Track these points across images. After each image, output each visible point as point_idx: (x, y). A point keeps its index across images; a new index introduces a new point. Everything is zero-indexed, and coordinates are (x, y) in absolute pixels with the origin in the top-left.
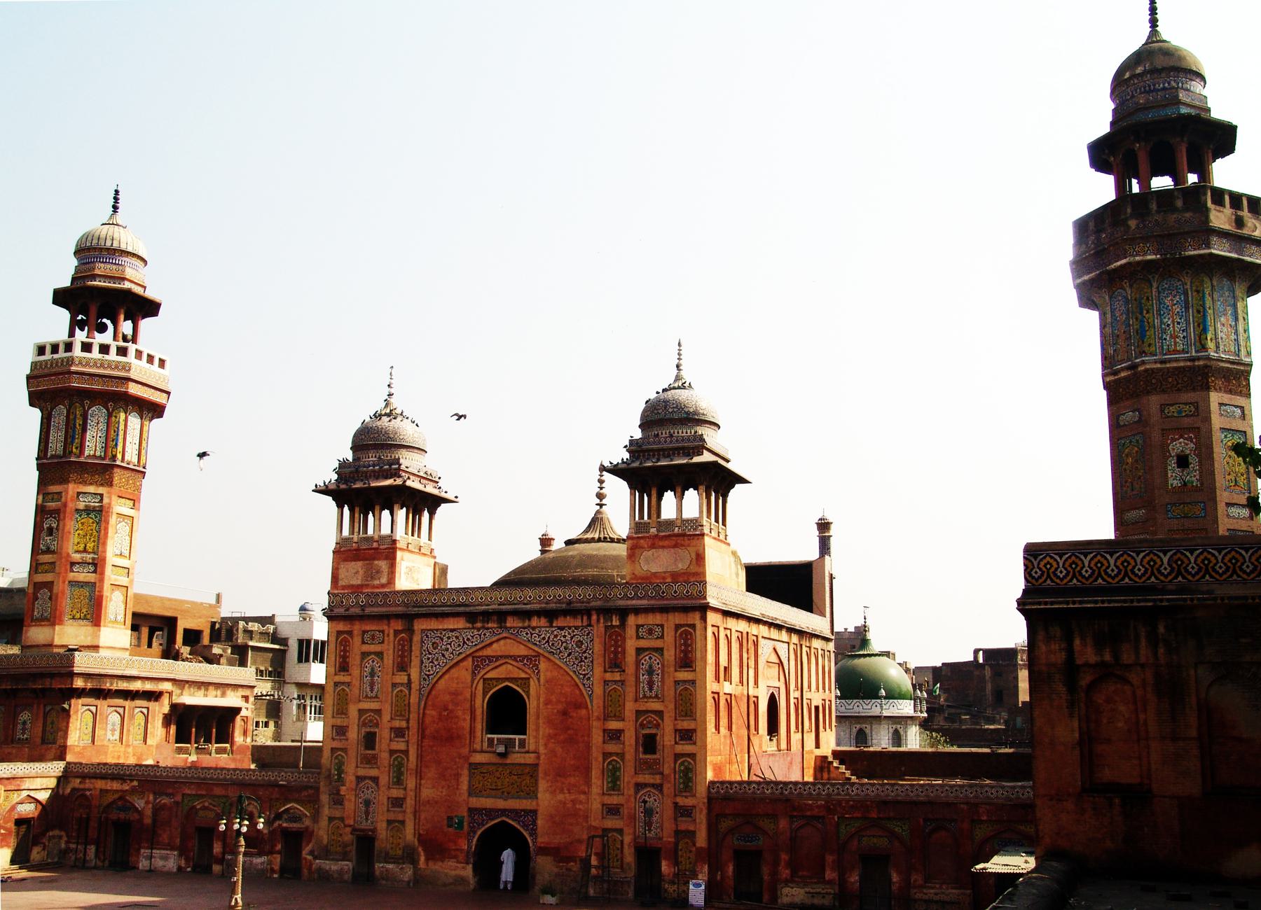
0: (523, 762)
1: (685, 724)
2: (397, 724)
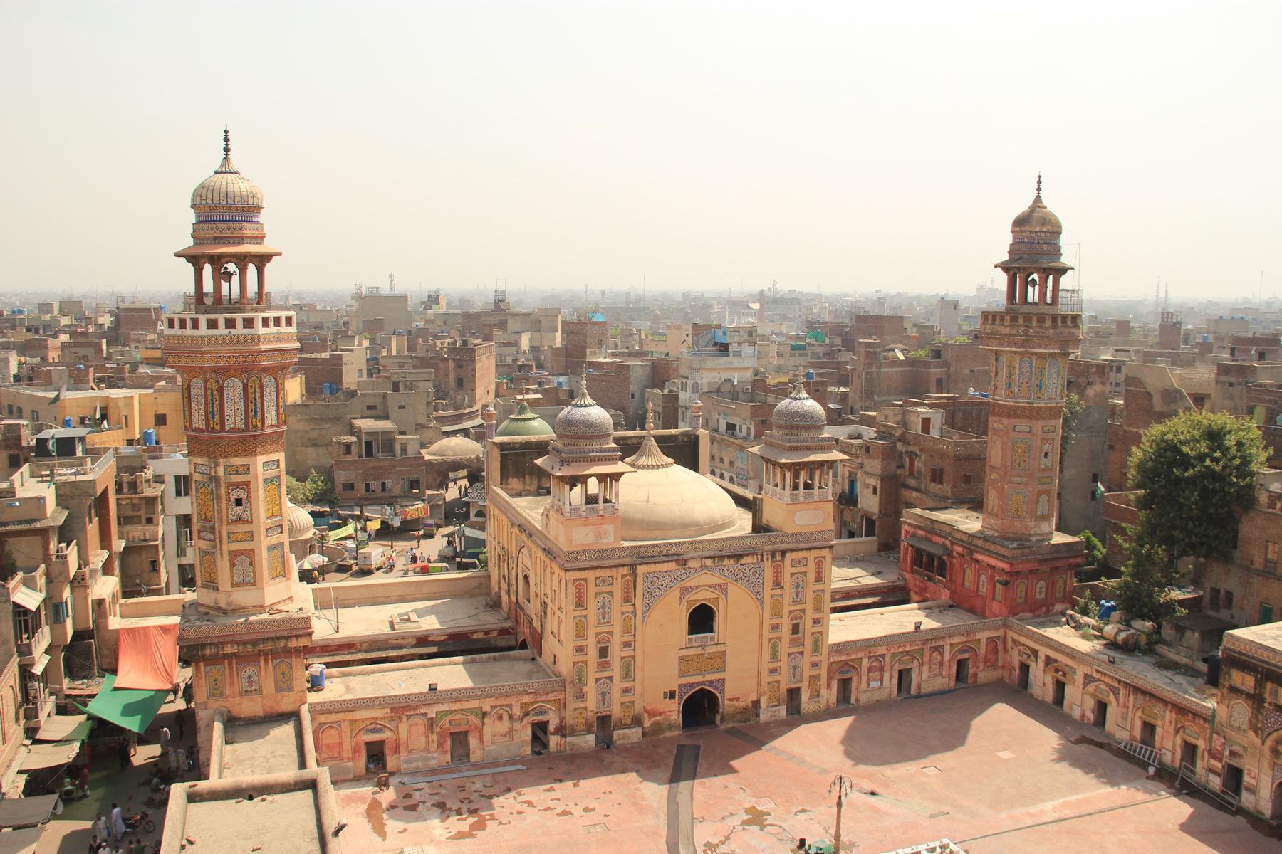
0: (716, 650)
1: (818, 616)
2: (626, 639)
